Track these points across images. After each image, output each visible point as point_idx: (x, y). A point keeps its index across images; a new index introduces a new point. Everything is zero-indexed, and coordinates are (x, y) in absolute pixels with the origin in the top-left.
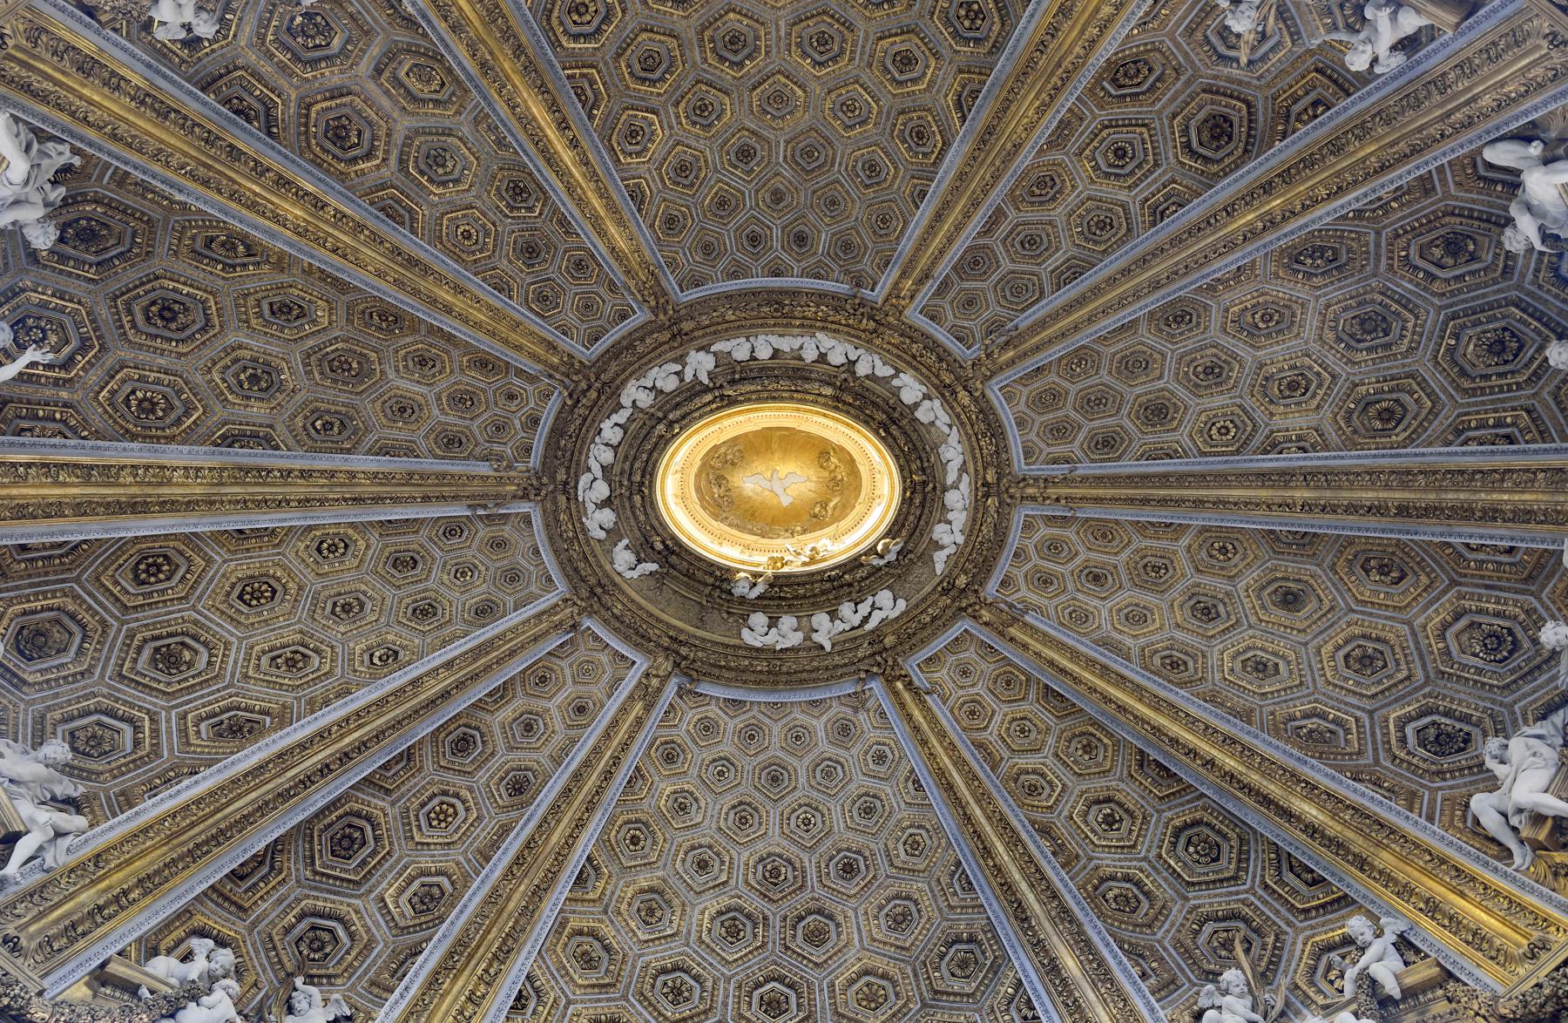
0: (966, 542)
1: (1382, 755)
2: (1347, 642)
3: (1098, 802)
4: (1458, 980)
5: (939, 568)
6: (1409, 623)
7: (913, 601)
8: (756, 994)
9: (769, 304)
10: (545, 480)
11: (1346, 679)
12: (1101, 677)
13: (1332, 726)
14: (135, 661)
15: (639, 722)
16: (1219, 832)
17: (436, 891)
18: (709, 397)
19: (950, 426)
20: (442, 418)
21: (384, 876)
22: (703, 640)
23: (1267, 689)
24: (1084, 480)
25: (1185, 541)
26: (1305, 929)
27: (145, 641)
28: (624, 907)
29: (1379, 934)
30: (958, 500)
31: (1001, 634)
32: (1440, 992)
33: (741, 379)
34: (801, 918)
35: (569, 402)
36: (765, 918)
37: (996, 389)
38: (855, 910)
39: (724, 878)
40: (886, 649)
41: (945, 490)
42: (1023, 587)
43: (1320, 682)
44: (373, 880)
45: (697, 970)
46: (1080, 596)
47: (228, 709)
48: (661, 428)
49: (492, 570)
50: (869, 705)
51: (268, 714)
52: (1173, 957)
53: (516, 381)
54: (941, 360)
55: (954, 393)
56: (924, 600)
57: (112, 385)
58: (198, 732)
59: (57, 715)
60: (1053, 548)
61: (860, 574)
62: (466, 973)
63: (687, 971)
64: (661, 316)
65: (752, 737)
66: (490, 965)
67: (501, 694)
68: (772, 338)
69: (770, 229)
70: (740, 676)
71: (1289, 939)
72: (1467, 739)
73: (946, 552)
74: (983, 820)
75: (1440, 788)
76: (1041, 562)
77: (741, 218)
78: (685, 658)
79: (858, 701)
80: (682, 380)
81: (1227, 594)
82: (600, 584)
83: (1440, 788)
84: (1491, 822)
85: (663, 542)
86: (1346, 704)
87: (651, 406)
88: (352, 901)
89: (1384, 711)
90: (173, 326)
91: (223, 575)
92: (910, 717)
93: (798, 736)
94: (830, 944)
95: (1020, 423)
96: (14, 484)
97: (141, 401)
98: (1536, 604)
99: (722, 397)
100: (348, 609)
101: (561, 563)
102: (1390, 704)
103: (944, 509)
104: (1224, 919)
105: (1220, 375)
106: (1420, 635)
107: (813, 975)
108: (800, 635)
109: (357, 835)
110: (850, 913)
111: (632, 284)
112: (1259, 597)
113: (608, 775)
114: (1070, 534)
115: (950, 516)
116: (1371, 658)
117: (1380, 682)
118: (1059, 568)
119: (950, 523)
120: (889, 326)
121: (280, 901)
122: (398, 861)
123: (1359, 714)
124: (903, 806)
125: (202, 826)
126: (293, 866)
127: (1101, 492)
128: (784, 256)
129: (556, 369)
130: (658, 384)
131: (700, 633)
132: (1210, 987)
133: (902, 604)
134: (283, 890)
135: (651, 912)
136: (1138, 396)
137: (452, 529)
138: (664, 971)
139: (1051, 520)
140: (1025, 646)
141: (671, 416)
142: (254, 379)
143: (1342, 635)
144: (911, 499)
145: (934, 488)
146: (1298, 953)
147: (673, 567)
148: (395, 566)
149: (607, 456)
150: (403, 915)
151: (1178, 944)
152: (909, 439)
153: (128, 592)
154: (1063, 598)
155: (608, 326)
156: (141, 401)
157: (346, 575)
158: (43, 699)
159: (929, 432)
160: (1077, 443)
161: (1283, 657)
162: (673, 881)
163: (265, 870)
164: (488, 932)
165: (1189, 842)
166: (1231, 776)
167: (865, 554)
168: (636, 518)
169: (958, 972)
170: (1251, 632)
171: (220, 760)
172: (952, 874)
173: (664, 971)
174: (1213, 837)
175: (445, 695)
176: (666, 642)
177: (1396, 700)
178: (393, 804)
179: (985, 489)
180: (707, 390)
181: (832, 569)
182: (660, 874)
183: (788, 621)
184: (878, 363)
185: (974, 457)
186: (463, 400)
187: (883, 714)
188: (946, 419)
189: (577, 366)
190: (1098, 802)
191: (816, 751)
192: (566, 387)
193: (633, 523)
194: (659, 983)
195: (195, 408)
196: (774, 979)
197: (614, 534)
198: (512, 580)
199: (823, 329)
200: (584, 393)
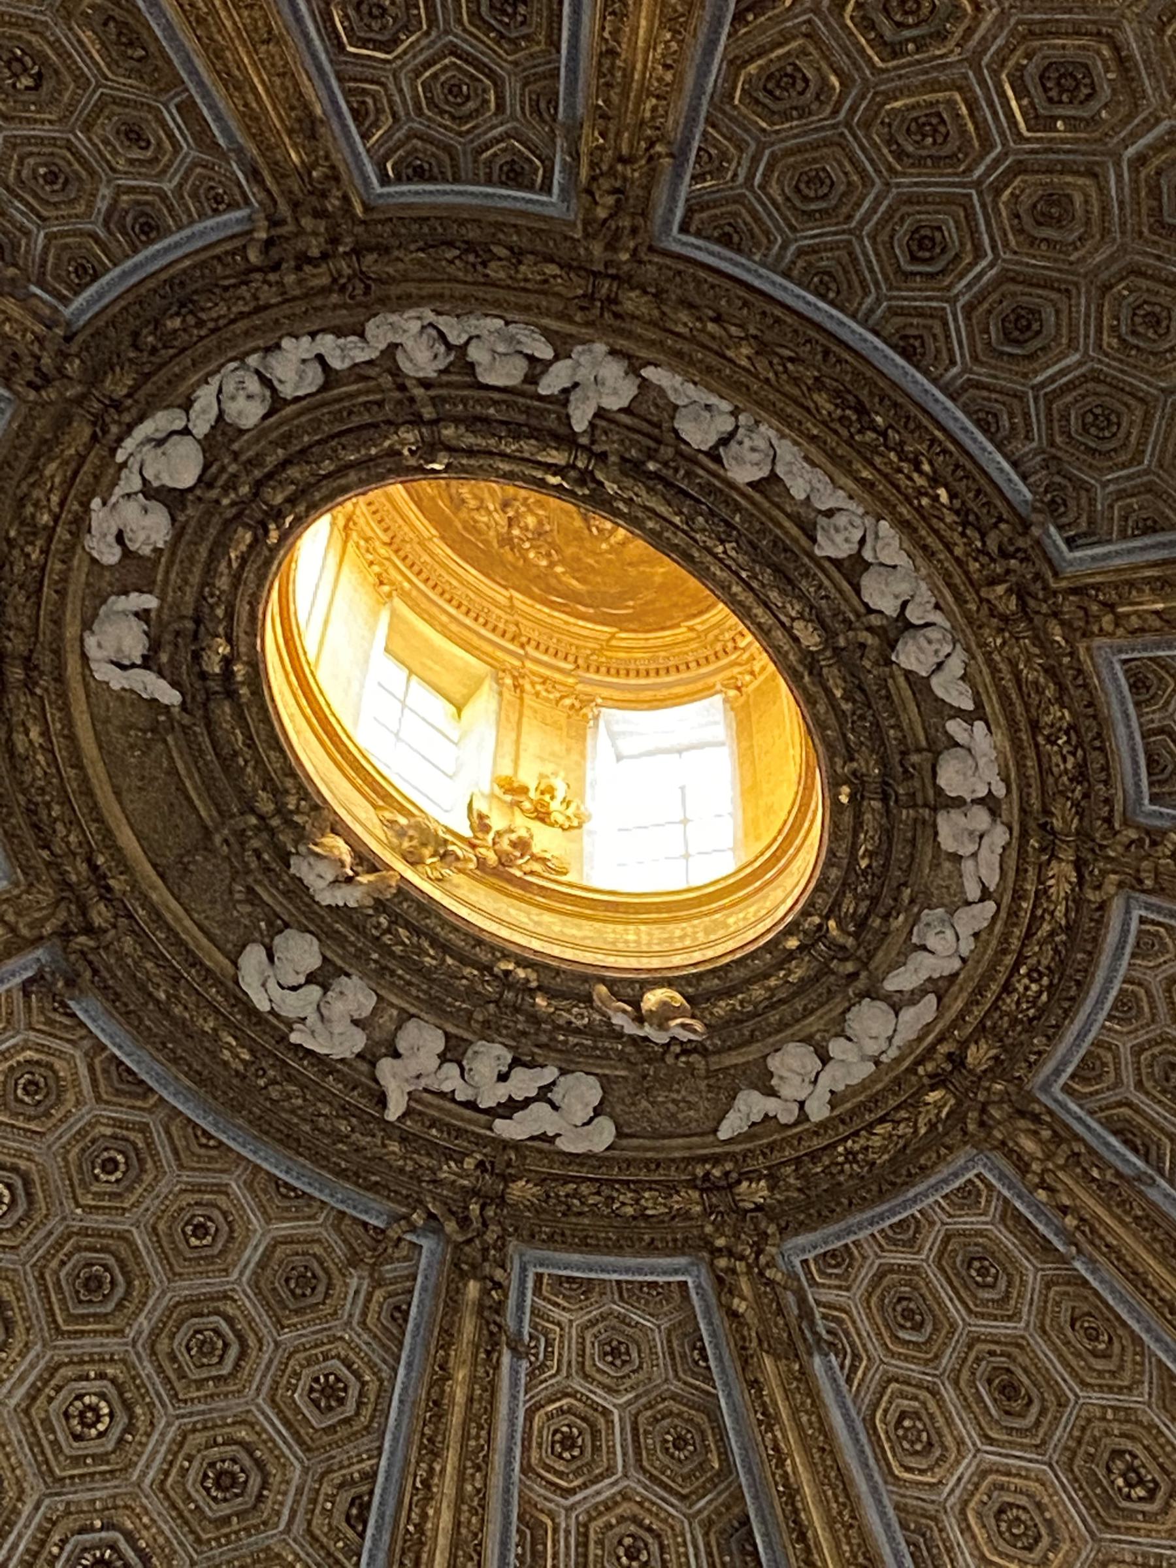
0: (824, 1125)
9: (837, 395)
10: (73, 368)
18: (557, 457)
19: (985, 895)
22: (156, 915)
33: (656, 476)
37: (1136, 913)
41: (872, 993)
46: (949, 1394)
53: (172, 118)
54: (1081, 774)
55: (1050, 851)
64: (597, 249)
65: (110, 1166)
68: (787, 451)
69: (979, 254)
73: (771, 1105)
76: (932, 1272)
77: (938, 183)
80: (532, 379)
82: (27, 662)
85: (227, 661)
87: (425, 384)
92: (444, 1374)
95: (1125, 1008)
99: (585, 477)
108: (358, 1041)
111: (590, 139)
114: (1032, 1272)
115: (836, 1047)
118: (955, 1310)
119: (825, 1059)
120: (1041, 640)
124: (299, 1527)
128: (958, 326)
129: (280, 171)
130: (475, 353)
131: (160, 894)
133: (603, 1136)
139: (1011, 1217)
140: (769, 1420)
141: (448, 432)
144: (791, 955)
145: (853, 976)
147: (209, 724)
152: (882, 852)
154: (914, 1371)
155: (465, 164)
159: (936, 866)
167: (610, 983)
168: (210, 570)
176: (77, 871)
180: (567, 440)
181: (523, 963)
184: (956, 666)
185: (980, 990)
187: (400, 1313)
189: (333, 203)
191: (215, 1283)
192: (274, 222)
193: (195, 579)
199: (903, 525)
200: (303, 259)
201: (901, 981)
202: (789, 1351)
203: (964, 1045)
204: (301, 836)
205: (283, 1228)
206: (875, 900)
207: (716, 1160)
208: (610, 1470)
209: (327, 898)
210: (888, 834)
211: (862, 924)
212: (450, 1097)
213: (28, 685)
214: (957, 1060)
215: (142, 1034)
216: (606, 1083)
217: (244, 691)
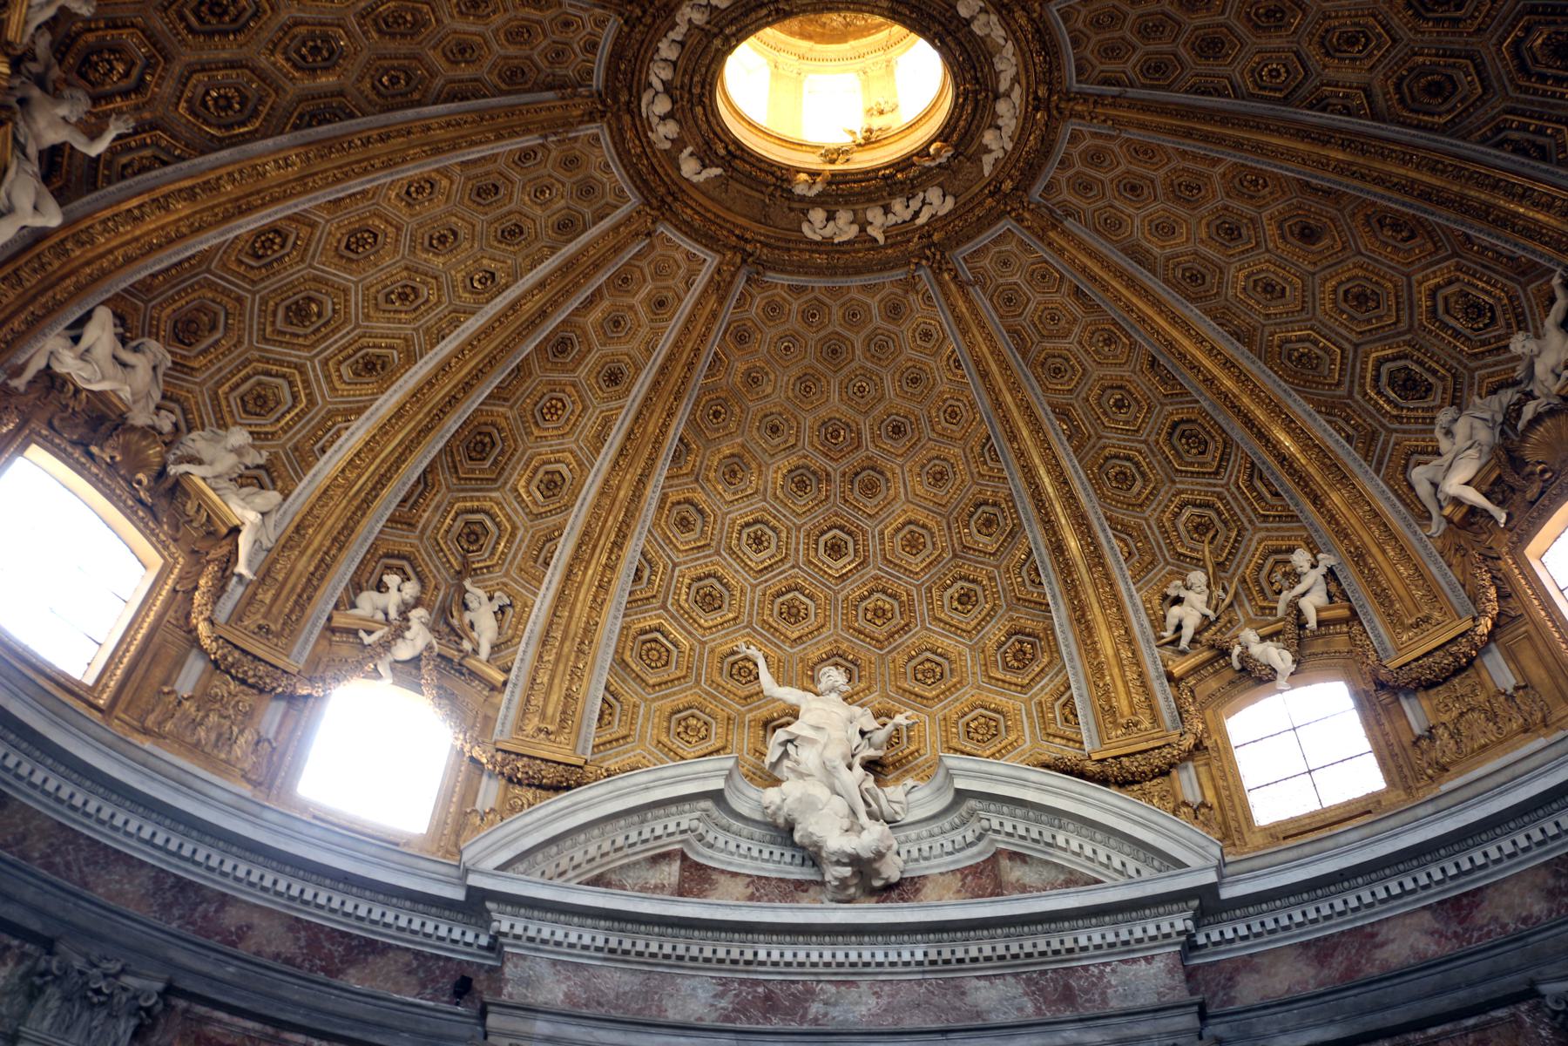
1: (1356, 388)
2: (1349, 280)
3: (1112, 387)
4: (1361, 624)
5: (987, 170)
6: (1408, 276)
7: (962, 200)
8: (822, 540)
11: (1343, 312)
12: (1127, 287)
13: (1320, 353)
14: (273, 323)
15: (714, 315)
16: (1209, 433)
17: (557, 478)
20: (502, 52)
21: (514, 469)
23: (1272, 311)
24: (1133, 105)
25: (1220, 169)
26: (1261, 529)
27: (277, 305)
28: (712, 475)
29: (1314, 566)
30: (1007, 112)
31: (1041, 239)
32: (1345, 629)
34: (857, 474)
35: (626, 29)
36: (828, 474)
38: (902, 467)
39: (792, 441)
40: (934, 244)
41: (997, 97)
42: (1065, 191)
43: (1319, 312)
44: (506, 474)
45: (773, 522)
47: (360, 349)
48: (717, 42)
49: (568, 185)
50: (919, 287)
51: (392, 348)
52: (1155, 535)
55: (1011, 11)
56: (970, 201)
57: (188, 94)
58: (341, 376)
59: (226, 388)
60: (1096, 158)
61: (913, 172)
62: (594, 562)
63: (766, 523)
65: (814, 316)
66: (611, 552)
67: (590, 302)
70: (802, 268)
71: (1247, 535)
72: (1429, 388)
73: (994, 155)
74: (1013, 407)
75: (1396, 431)
78: (751, 255)
79: (910, 285)
81: (1251, 220)
83: (1396, 431)
84: (1423, 490)
85: (726, 148)
86: (1337, 334)
87: (708, 23)
88: (493, 494)
89: (1367, 348)
90: (227, 19)
91: (330, 233)
93: (854, 316)
94: (881, 497)
95: (1076, 42)
96: (134, 228)
97: (215, 100)
98: (1521, 293)
99: (777, 11)
100: (443, 240)
101: (631, 177)
102: (1374, 341)
103: (995, 115)
104: (1200, 506)
105: (1281, 19)
106: (1415, 289)
107: (867, 524)
108: (855, 229)
109: (487, 440)
110: (898, 470)
112: (1280, 227)
113: (690, 366)
115: (1000, 122)
116: (1367, 299)
117: (1369, 321)
119: (999, 128)
121: (437, 507)
122: (523, 454)
123: (1346, 345)
125: (367, 474)
126: (444, 477)
127: (1147, 118)
132: (1179, 583)
133: (950, 203)
134: (437, 498)
135: (733, 473)
136: (1197, 28)
137: (526, 155)
138: (748, 525)
139: (1095, 135)
142: (315, 50)
143: (1347, 275)
144: (963, 105)
146: (1252, 548)
148: (479, 195)
149: (667, 74)
150: (535, 503)
151: (1161, 527)
152: (964, 50)
153: (252, 268)
156: (215, 100)
157: (434, 209)
158: (211, 376)
160: (1130, 64)
161: (1290, 283)
162: (749, 445)
163: (421, 487)
164: (606, 521)
165: (1182, 435)
166: (1224, 396)
167: (917, 154)
169: (984, 530)
170: (1267, 256)
171: (366, 408)
172: (983, 447)
173: (748, 525)
174: (1203, 435)
175: (543, 314)
177: (1380, 340)
178: (511, 408)
179: (1035, 103)
181: (886, 168)
182: (739, 440)
183: (844, 216)
185: (1027, 71)
186: (520, 34)
187: (930, 298)
188: (1002, 33)
190: (1112, 387)
191: (871, 327)
192: (621, 15)
194: (744, 536)
195: (268, 95)
196: (835, 527)
197: (679, 144)
198: (588, 192)
200: (639, 19)
201: (1003, 86)
202: (1054, 227)
203: (1036, 92)
204: (789, 182)
205: (878, 297)
206: (974, 68)
207: (989, 184)
208: (1029, 300)
209: (812, 193)
210: (960, 44)
211: (977, 79)
212: (896, 224)
213: (676, 199)
214: (1036, 98)
215: (791, 273)
216: (941, 185)
217: (738, 153)
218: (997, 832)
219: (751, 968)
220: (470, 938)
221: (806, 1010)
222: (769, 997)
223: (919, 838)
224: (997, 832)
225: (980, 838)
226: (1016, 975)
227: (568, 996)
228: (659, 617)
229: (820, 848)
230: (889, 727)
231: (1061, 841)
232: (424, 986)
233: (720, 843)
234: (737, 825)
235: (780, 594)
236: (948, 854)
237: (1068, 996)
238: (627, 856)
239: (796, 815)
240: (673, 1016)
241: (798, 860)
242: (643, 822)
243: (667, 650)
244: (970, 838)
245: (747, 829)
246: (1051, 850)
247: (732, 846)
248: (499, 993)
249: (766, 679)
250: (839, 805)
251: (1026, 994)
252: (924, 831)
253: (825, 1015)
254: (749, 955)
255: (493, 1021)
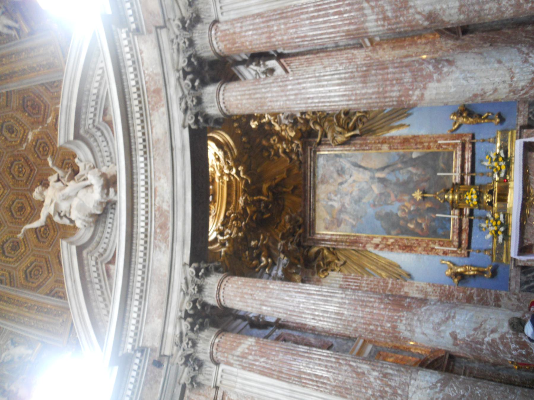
218: (94, 121)
219: (149, 235)
220: (137, 361)
221: (166, 211)
222: (161, 227)
223: (102, 156)
224: (94, 121)
225: (99, 129)
226: (150, 115)
227: (159, 317)
228: (19, 271)
229: (101, 203)
230: (55, 168)
231: (95, 91)
232: (157, 381)
233: (104, 246)
234: (97, 239)
235: (12, 215)
236: (108, 143)
237: (157, 91)
238: (106, 289)
239: (87, 213)
240: (166, 271)
241: (112, 211)
242: (91, 282)
243: (35, 266)
244: (99, 134)
245: (99, 234)
246: (100, 97)
247: (106, 241)
248: (156, 348)
249: (36, 224)
250: (82, 193)
251: (157, 111)
252: (99, 154)
253: (167, 202)
254: (143, 236)
255: (167, 352)
